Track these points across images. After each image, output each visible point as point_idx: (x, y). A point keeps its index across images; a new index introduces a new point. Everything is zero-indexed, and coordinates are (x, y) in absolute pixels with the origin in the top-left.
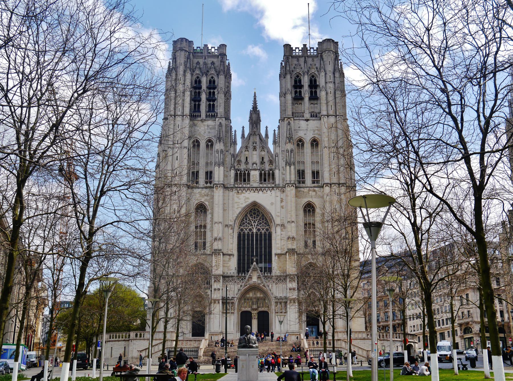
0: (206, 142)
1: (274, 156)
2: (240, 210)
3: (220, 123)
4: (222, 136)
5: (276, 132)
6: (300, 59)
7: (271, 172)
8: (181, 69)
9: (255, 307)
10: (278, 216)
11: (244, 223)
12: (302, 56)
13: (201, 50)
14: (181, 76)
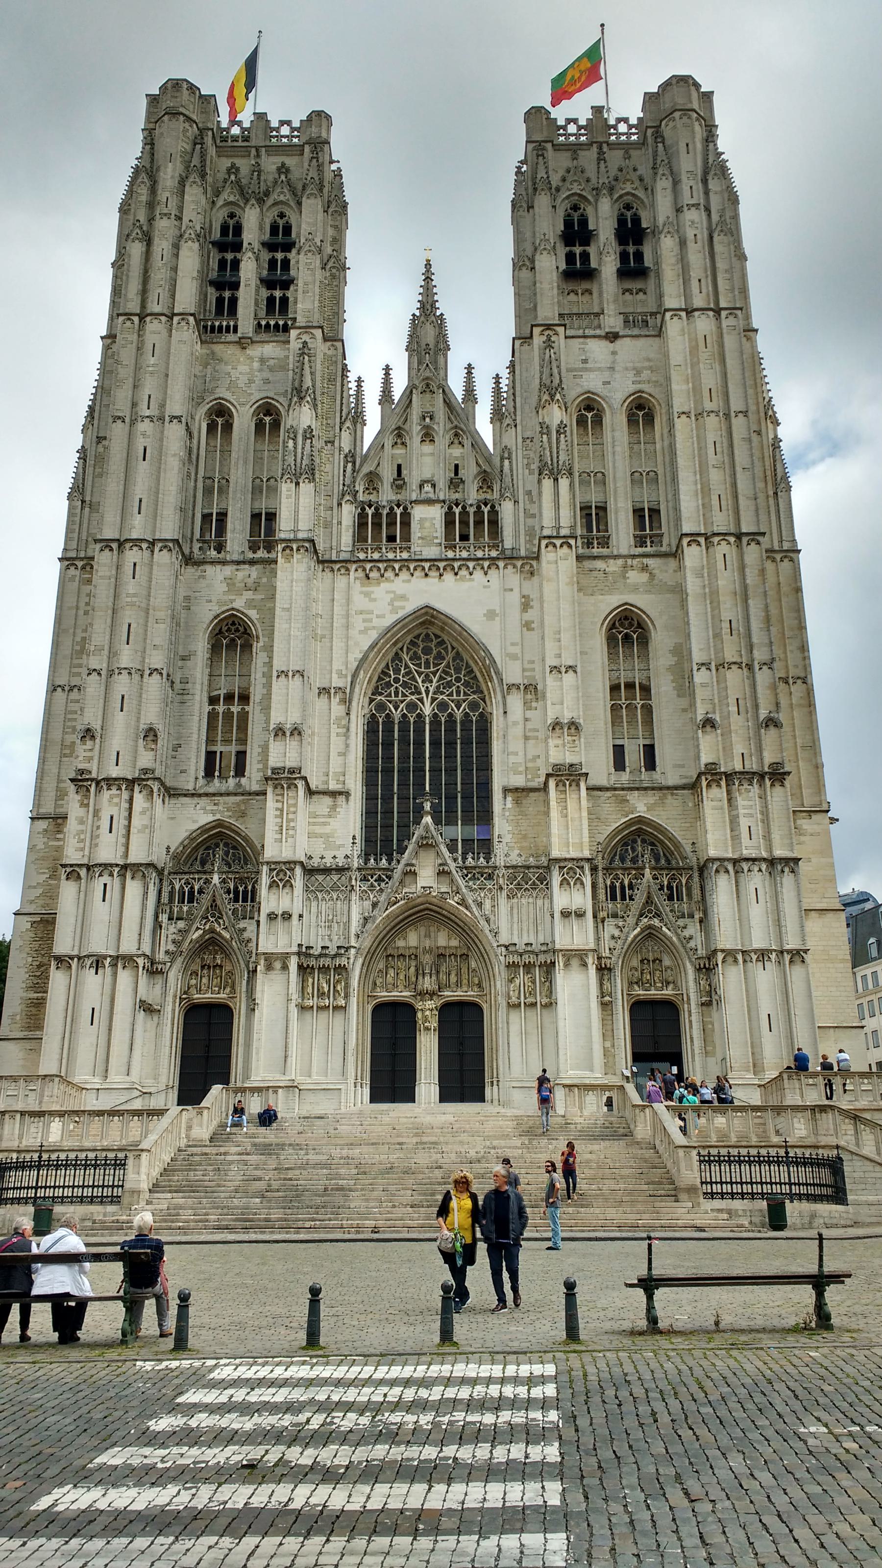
0: (256, 413)
1: (497, 461)
2: (374, 635)
3: (305, 343)
4: (308, 382)
5: (504, 382)
6: (581, 153)
7: (486, 510)
8: (169, 175)
9: (428, 983)
10: (514, 657)
11: (389, 684)
12: (590, 144)
13: (243, 130)
14: (168, 194)
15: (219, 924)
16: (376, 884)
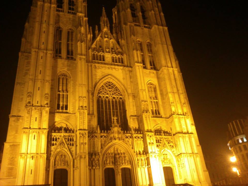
15: (64, 147)
16: (104, 138)
